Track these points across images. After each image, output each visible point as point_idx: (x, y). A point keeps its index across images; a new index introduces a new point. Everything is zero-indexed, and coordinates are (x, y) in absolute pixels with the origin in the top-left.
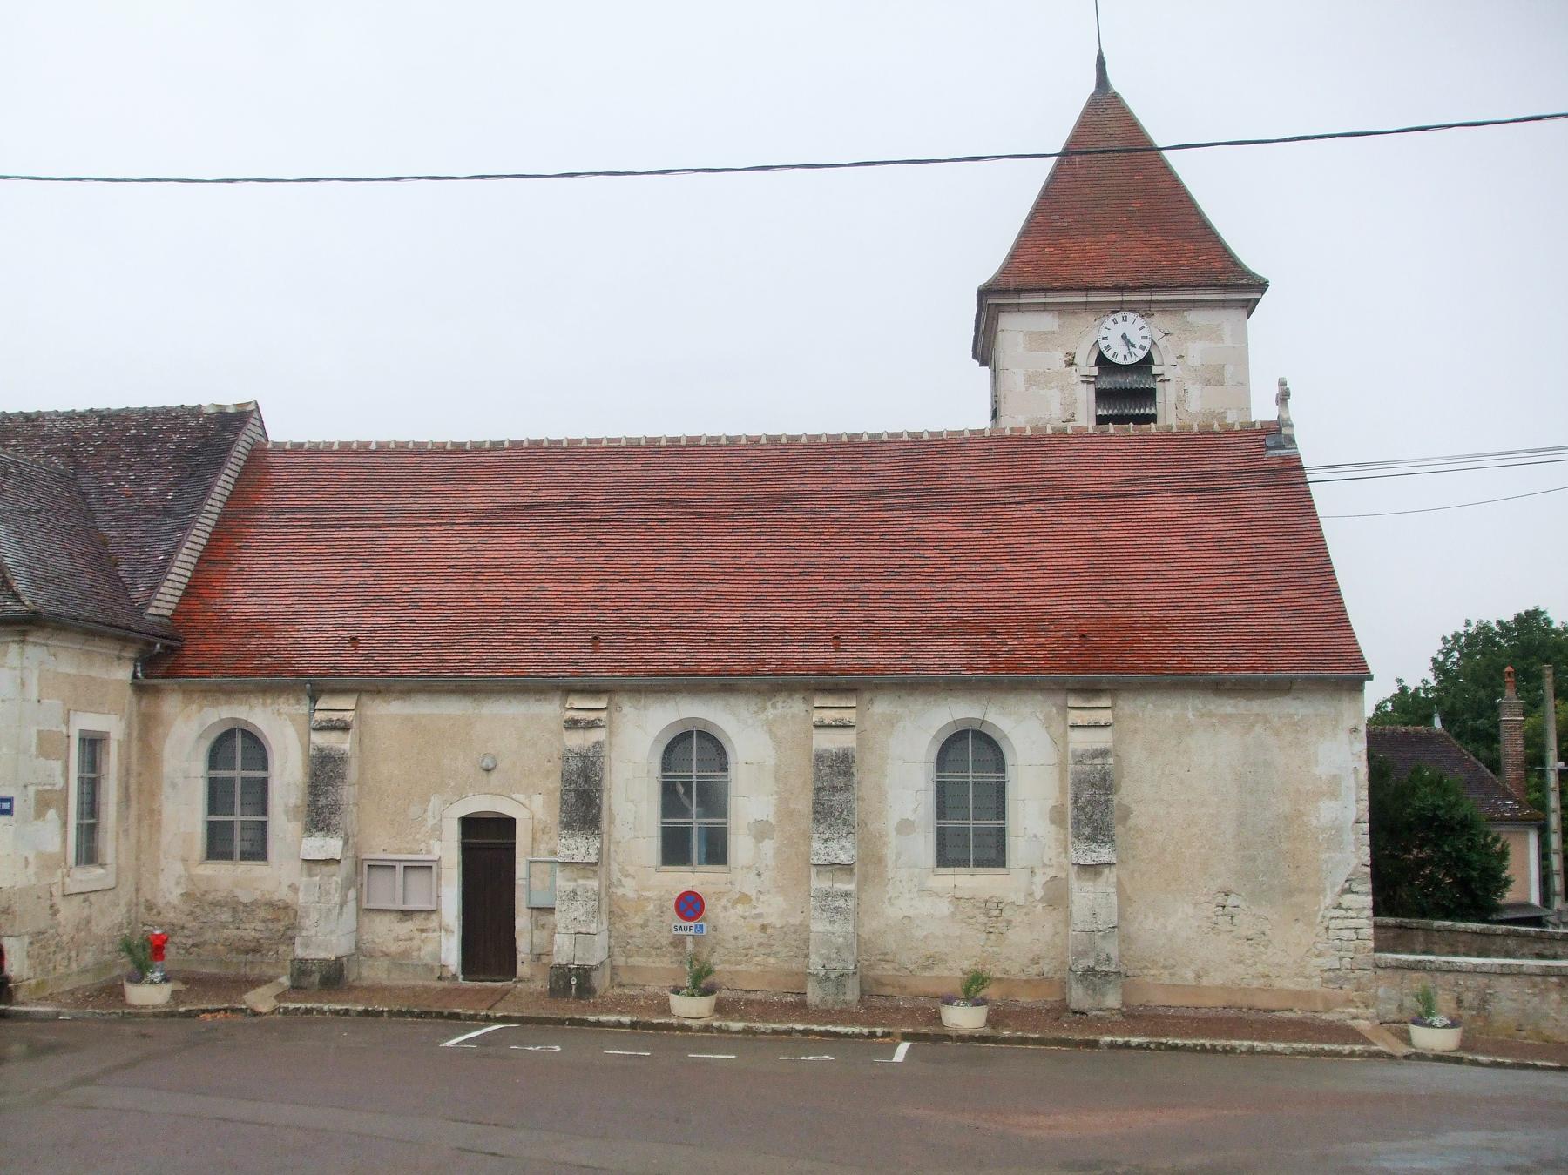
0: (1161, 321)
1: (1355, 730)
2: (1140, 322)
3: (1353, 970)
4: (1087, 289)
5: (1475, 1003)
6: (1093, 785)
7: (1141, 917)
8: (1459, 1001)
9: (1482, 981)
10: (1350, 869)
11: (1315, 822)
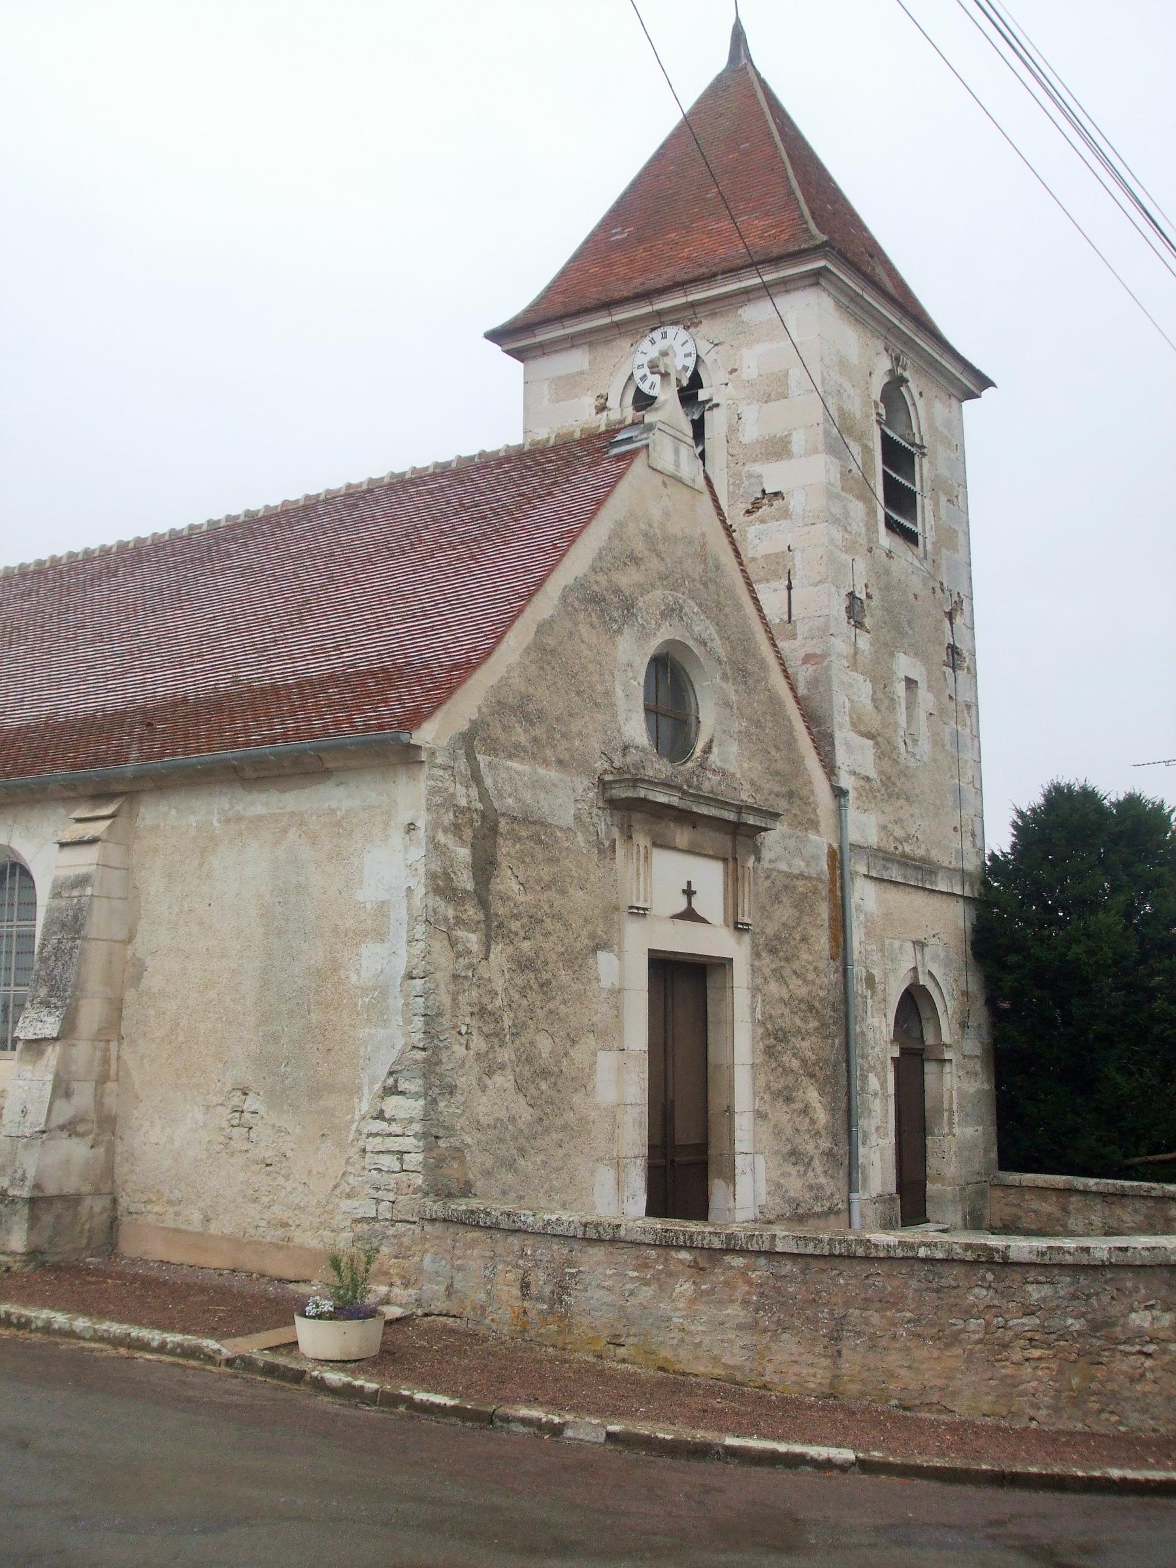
0: (710, 328)
1: (411, 827)
2: (683, 335)
3: (394, 1222)
4: (608, 305)
5: (548, 1290)
6: (63, 925)
7: (147, 1125)
8: (525, 1285)
9: (559, 1250)
10: (393, 1055)
11: (354, 979)
